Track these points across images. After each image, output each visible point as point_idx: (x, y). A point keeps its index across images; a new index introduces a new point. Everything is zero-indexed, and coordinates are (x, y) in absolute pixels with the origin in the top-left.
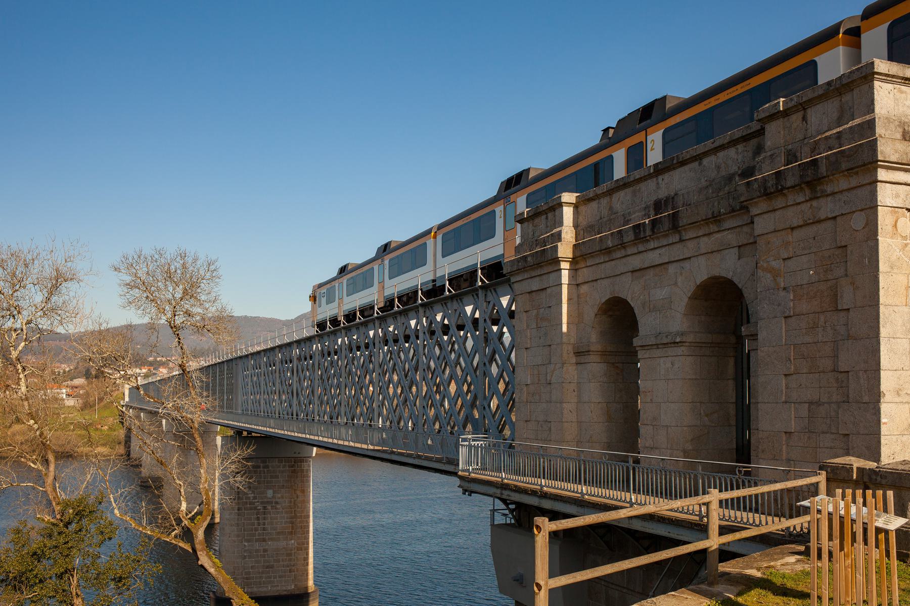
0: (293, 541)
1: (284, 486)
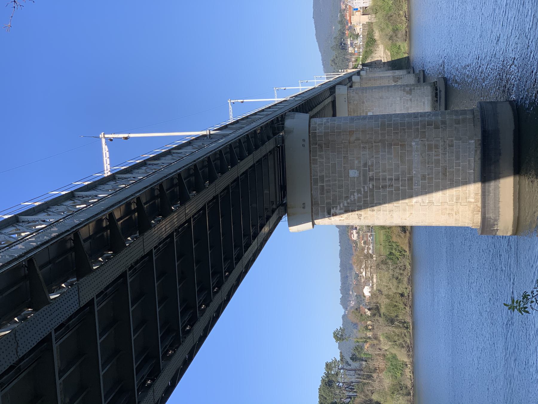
0: (413, 144)
1: (344, 157)
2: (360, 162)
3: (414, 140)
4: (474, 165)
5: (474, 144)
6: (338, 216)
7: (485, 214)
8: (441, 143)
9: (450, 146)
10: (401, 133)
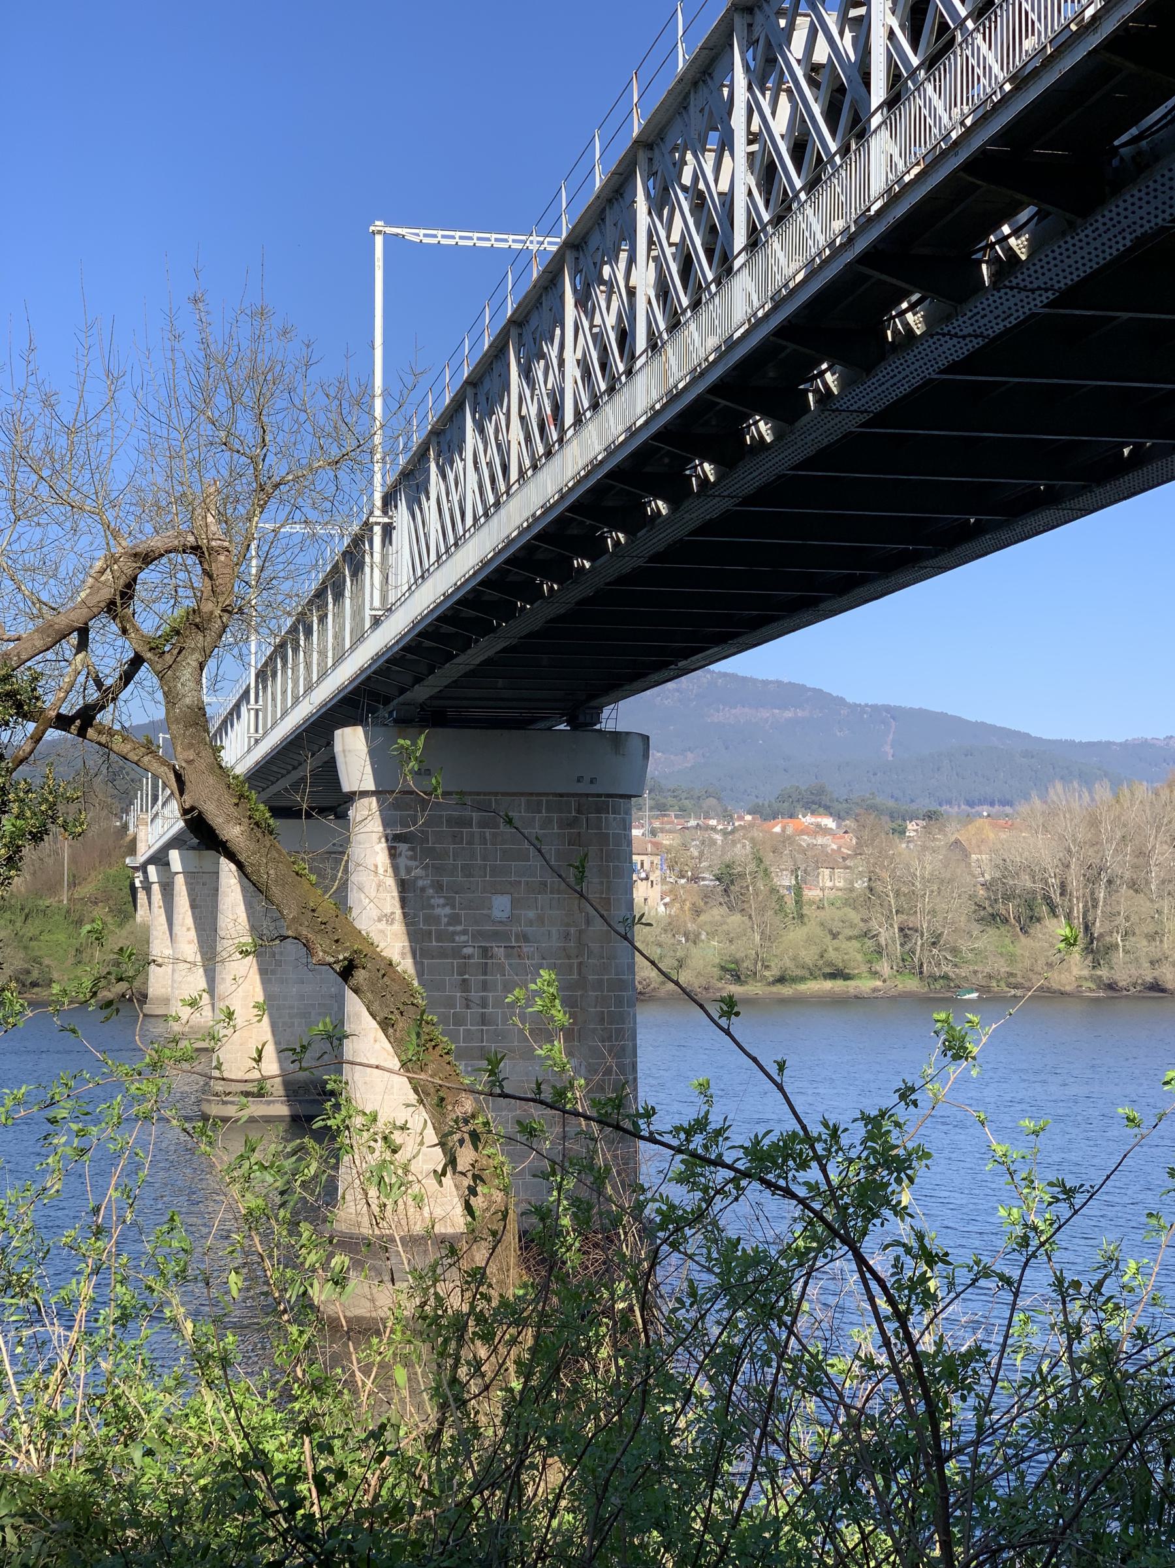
2: (530, 923)
6: (388, 861)
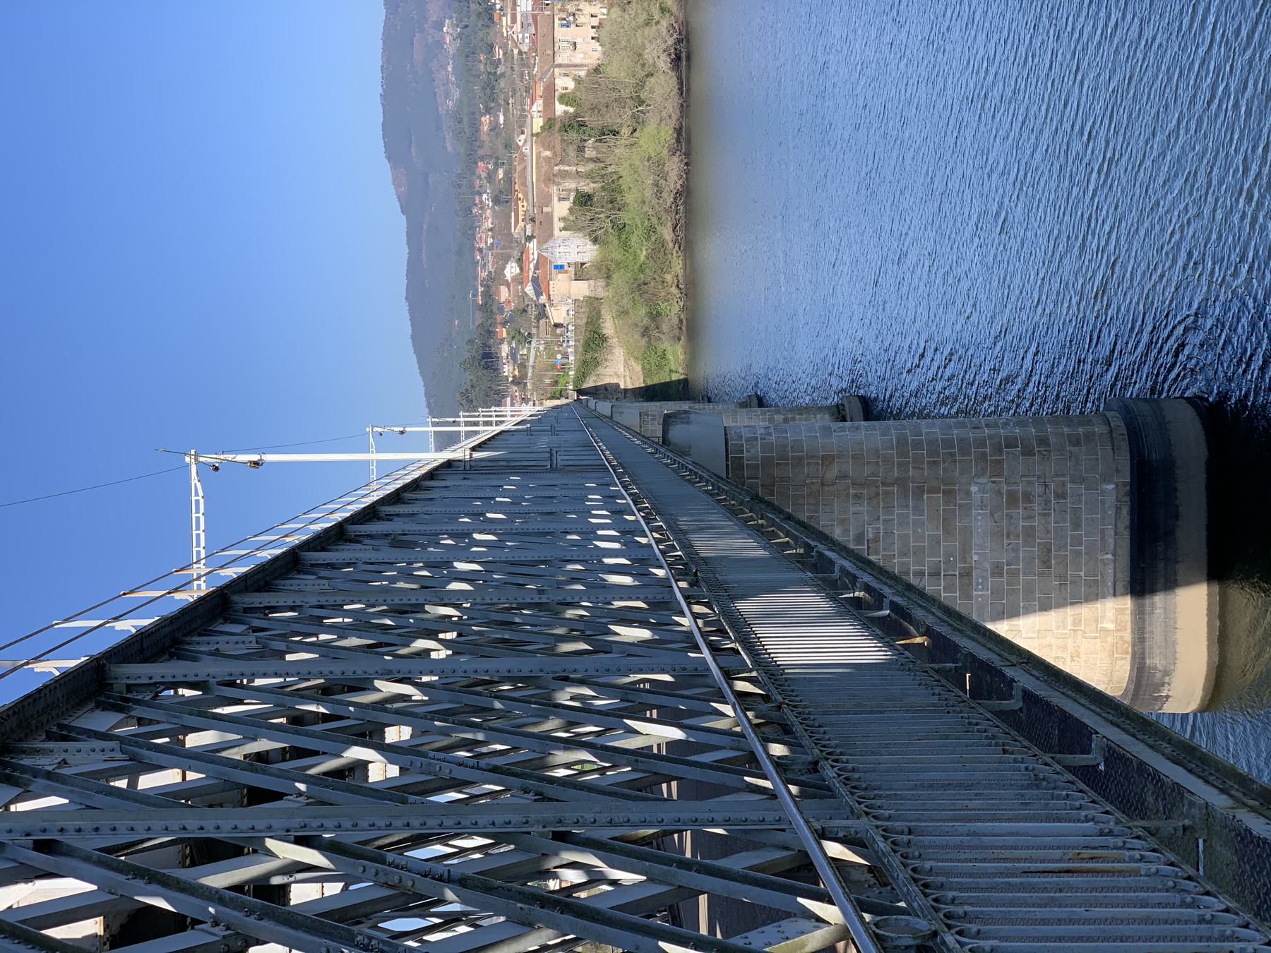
0: (974, 489)
2: (846, 531)
3: (975, 480)
4: (1115, 543)
5: (1114, 493)
7: (1144, 658)
8: (1038, 489)
9: (1058, 496)
10: (944, 462)
